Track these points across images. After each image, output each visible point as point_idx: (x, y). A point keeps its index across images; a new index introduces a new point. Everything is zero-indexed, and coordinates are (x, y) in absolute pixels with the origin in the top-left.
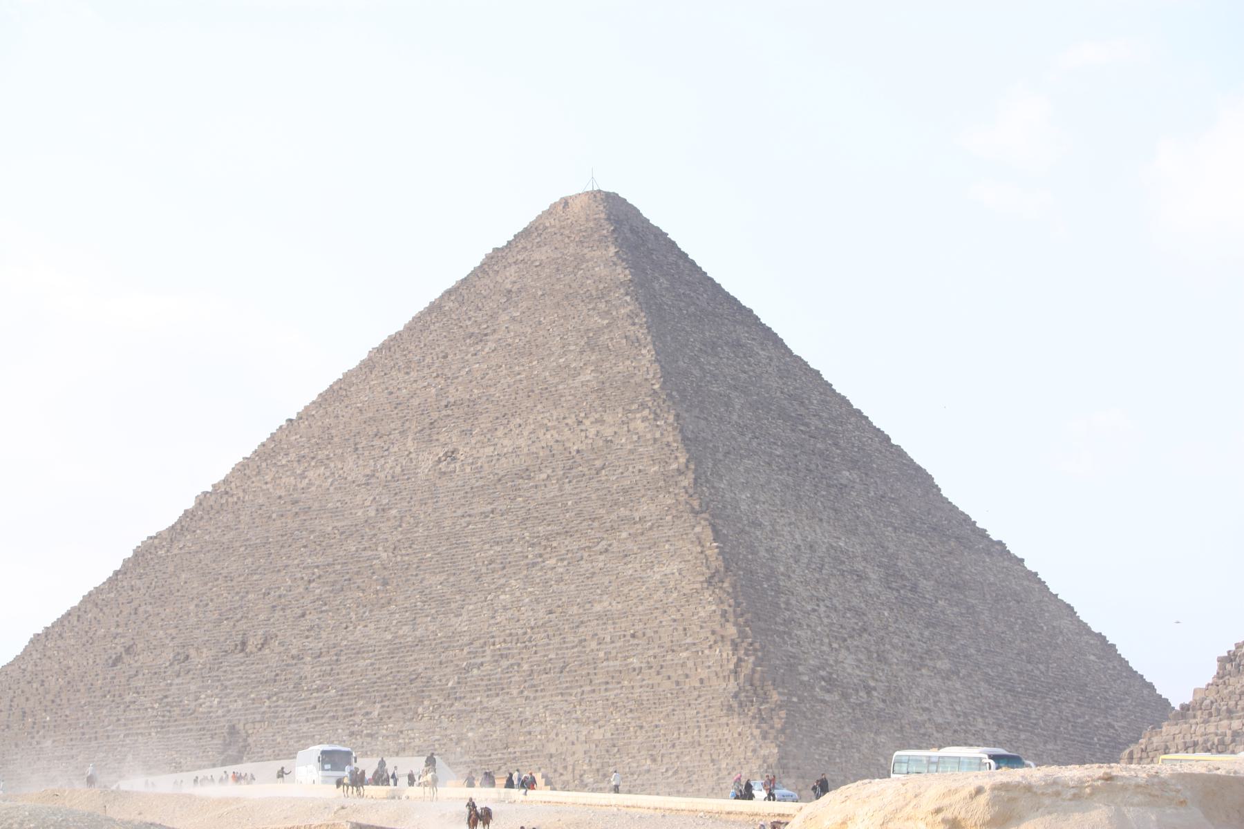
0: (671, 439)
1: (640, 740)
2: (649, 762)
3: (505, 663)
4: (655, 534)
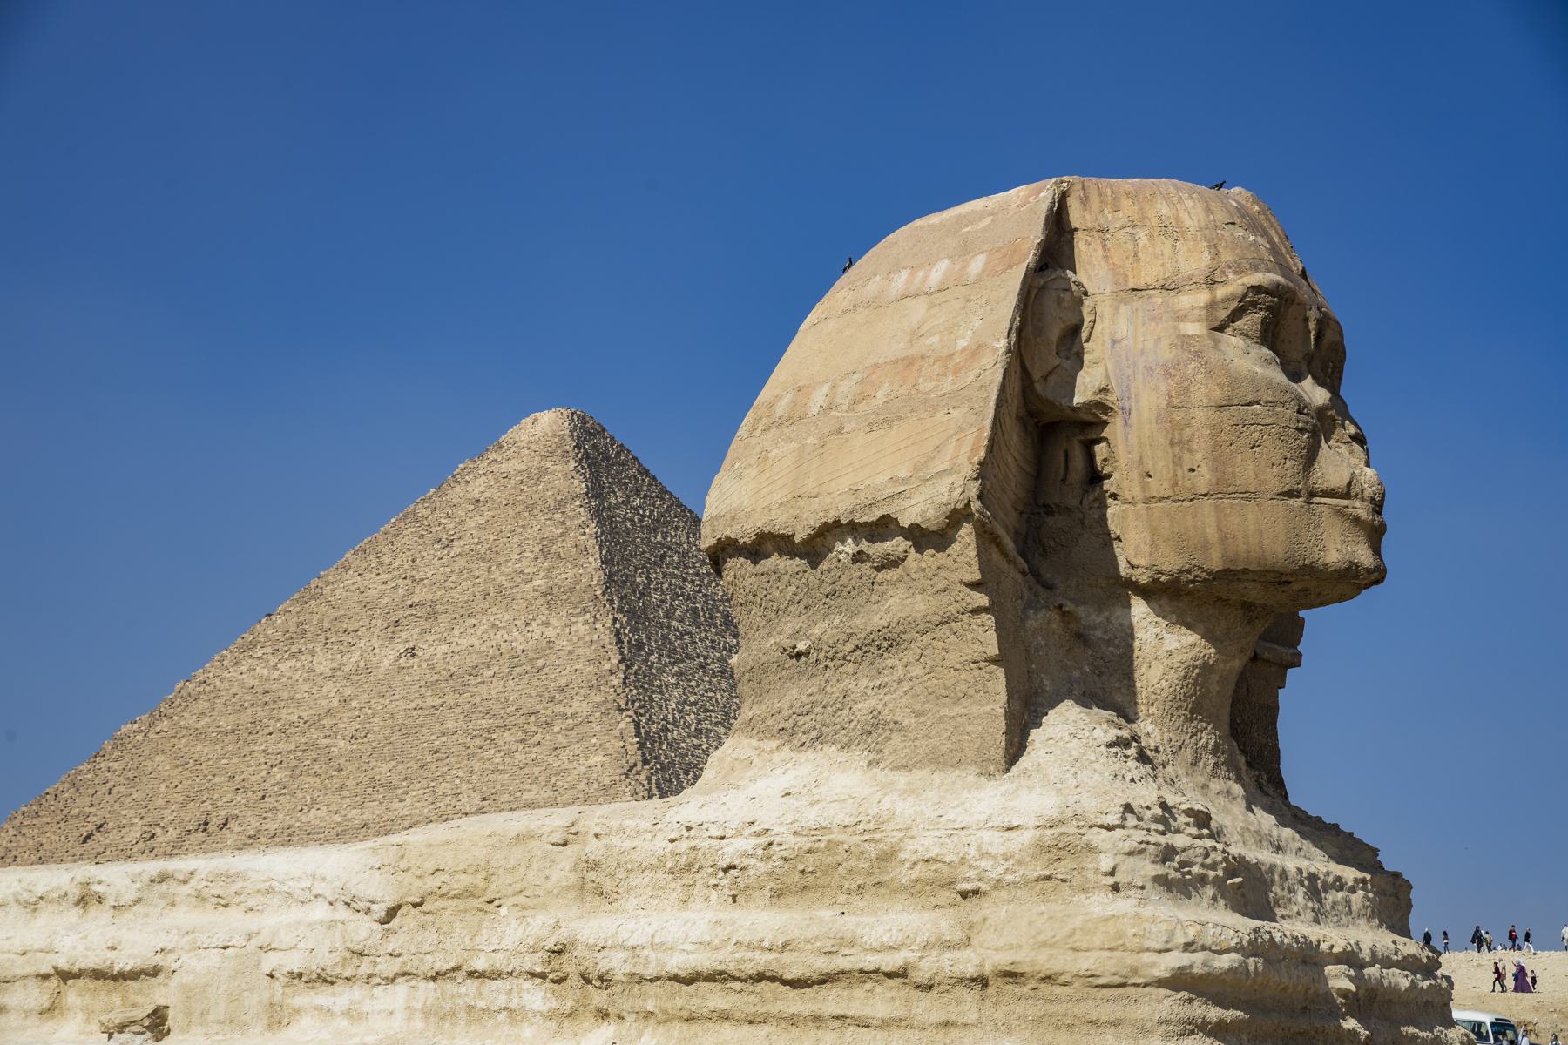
0: (607, 641)
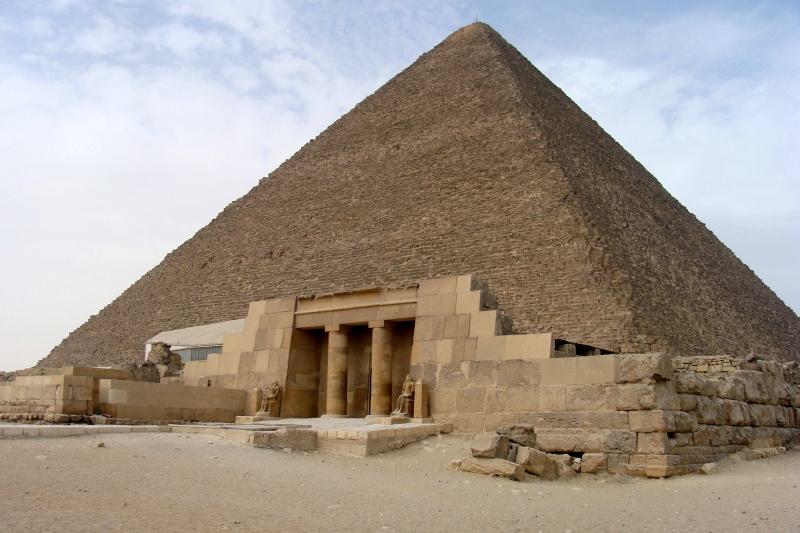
1: (520, 305)
2: (528, 322)
3: (424, 257)
4: (523, 176)
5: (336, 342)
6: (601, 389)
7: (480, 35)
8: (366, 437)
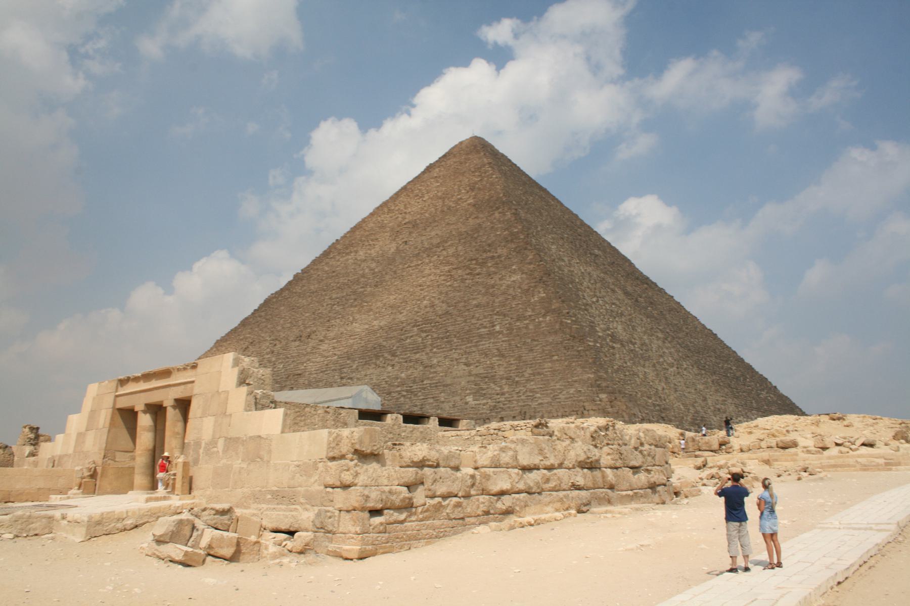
1: (501, 373)
3: (424, 335)
5: (145, 421)
6: (315, 466)
7: (475, 146)
8: (86, 519)
